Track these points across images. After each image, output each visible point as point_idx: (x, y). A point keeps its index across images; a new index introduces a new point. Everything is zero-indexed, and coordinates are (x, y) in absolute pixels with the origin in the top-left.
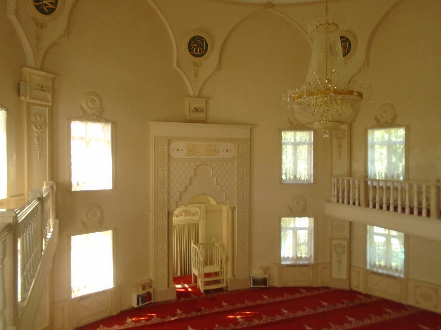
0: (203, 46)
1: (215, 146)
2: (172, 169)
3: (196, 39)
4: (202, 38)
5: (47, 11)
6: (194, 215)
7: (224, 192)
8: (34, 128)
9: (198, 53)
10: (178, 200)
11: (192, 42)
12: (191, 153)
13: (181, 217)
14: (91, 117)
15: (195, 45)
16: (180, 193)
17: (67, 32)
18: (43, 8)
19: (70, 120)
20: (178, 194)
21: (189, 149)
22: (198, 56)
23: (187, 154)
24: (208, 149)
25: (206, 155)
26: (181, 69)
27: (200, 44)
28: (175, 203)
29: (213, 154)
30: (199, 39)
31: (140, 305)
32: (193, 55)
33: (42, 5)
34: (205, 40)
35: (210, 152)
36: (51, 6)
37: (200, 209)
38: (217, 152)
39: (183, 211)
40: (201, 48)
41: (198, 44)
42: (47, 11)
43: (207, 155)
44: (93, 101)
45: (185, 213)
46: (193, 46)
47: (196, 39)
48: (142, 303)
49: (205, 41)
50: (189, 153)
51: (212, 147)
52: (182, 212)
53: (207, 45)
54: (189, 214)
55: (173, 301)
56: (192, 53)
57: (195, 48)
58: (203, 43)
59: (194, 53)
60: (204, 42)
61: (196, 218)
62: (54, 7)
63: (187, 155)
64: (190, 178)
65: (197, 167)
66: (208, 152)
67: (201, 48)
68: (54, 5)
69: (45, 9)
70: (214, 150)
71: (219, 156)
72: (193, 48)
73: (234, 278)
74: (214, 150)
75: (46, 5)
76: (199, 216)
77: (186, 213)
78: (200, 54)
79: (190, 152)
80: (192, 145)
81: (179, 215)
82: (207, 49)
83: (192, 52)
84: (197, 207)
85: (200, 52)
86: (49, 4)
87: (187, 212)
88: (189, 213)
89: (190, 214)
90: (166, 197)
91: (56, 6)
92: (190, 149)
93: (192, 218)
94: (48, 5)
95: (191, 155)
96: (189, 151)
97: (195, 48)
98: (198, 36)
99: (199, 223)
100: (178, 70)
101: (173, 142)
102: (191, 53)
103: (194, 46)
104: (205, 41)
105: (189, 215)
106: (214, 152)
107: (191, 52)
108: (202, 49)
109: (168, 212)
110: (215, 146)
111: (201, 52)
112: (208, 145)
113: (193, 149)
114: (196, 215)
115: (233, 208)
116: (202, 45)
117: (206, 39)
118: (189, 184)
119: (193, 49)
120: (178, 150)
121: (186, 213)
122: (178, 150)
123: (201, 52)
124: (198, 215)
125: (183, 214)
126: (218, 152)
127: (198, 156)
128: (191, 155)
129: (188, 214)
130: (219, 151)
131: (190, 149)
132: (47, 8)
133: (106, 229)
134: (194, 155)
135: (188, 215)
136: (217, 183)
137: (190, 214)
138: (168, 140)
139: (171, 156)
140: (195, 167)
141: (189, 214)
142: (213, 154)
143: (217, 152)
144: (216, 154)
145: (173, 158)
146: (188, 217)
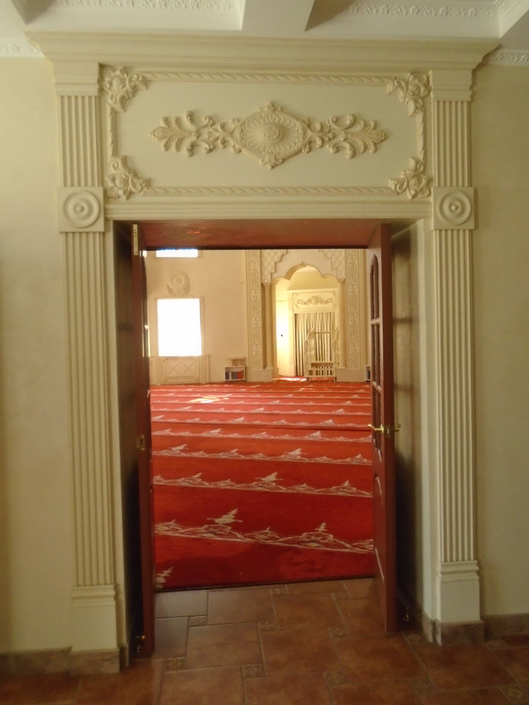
6: (327, 302)
10: (273, 271)
16: (276, 263)
20: (273, 264)
31: (230, 379)
39: (313, 297)
45: (315, 300)
48: (233, 378)
52: (311, 299)
54: (320, 301)
61: (330, 306)
73: (344, 368)
76: (333, 304)
77: (317, 299)
87: (318, 299)
88: (321, 300)
89: (322, 301)
90: (258, 267)
99: (334, 313)
105: (320, 302)
109: (262, 285)
114: (329, 302)
115: (343, 281)
121: (317, 299)
124: (332, 302)
129: (319, 301)
133: (193, 297)
135: (319, 302)
137: (322, 301)
141: (320, 301)
146: (319, 305)
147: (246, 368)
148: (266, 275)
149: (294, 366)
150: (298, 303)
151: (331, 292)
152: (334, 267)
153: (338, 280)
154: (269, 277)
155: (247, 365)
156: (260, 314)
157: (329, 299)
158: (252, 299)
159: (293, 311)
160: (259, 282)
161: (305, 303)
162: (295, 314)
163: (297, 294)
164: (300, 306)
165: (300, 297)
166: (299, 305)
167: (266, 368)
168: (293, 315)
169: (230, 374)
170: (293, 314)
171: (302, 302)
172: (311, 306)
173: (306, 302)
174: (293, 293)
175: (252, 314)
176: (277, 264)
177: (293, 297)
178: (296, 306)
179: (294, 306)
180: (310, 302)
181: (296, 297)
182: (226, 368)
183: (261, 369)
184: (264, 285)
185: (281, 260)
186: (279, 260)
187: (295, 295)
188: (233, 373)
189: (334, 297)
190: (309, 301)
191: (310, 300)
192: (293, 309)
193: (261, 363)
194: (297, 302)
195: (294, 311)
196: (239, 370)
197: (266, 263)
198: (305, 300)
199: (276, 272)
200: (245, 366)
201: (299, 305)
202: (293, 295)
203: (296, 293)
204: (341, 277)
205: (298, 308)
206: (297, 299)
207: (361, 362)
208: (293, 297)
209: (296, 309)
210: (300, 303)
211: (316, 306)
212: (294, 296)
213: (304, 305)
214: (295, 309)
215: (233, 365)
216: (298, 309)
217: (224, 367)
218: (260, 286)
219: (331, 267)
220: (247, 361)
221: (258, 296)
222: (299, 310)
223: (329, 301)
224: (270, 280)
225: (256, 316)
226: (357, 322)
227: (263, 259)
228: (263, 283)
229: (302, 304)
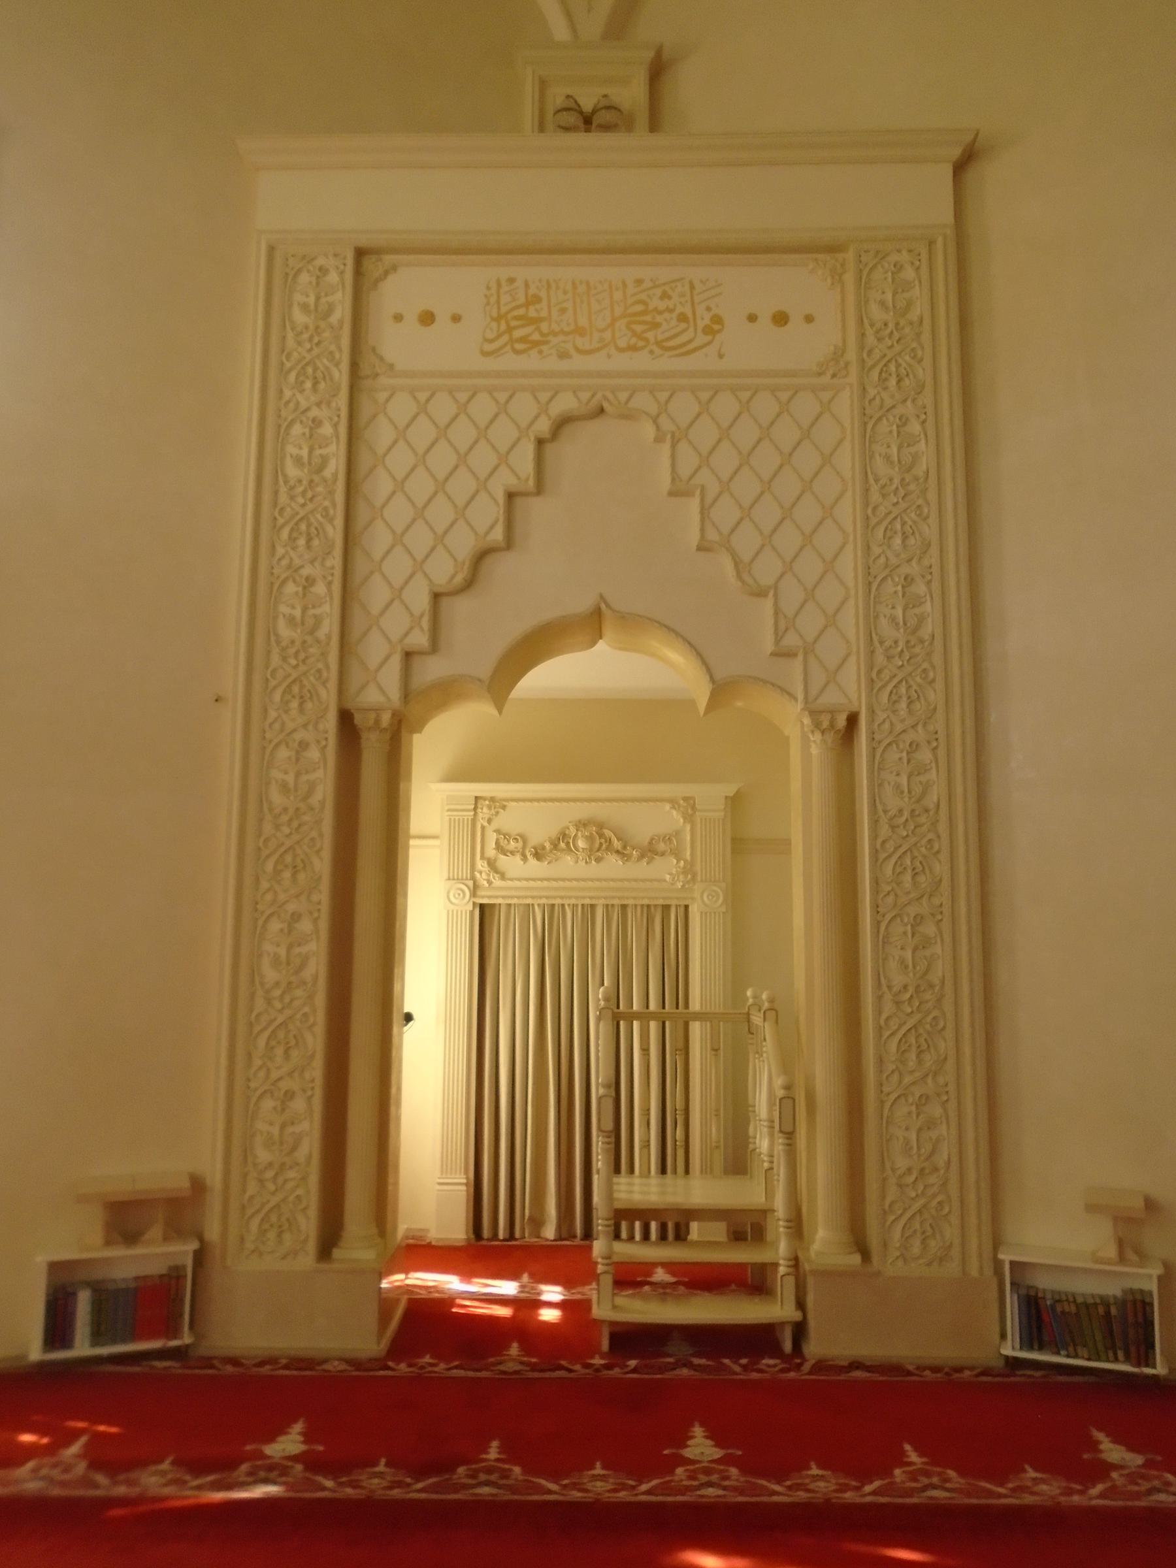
1: (692, 287)
2: (381, 434)
6: (649, 851)
7: (768, 603)
10: (419, 639)
12: (517, 334)
13: (569, 859)
16: (436, 597)
20: (420, 601)
21: (504, 310)
23: (491, 341)
24: (640, 308)
25: (621, 350)
28: (396, 662)
29: (671, 343)
35: (655, 325)
37: (689, 818)
38: (707, 330)
39: (582, 824)
43: (633, 348)
45: (590, 839)
48: (97, 1337)
50: (506, 338)
51: (665, 296)
52: (573, 832)
54: (617, 844)
55: (335, 1366)
61: (666, 869)
63: (488, 347)
64: (511, 496)
65: (562, 424)
66: (638, 328)
70: (682, 318)
71: (721, 356)
74: (682, 318)
76: (682, 863)
77: (601, 835)
79: (510, 330)
80: (527, 285)
81: (555, 846)
84: (667, 806)
87: (607, 833)
89: (625, 847)
90: (329, 612)
92: (515, 313)
93: (640, 869)
95: (519, 346)
96: (503, 327)
99: (687, 907)
101: (395, 268)
105: (618, 852)
106: (683, 325)
109: (346, 719)
110: (692, 287)
112: (639, 282)
113: (532, 313)
114: (663, 854)
115: (841, 722)
118: (498, 535)
120: (428, 318)
121: (601, 835)
122: (428, 318)
124: (677, 854)
125: (581, 844)
126: (716, 327)
127: (563, 355)
128: (518, 352)
130: (717, 319)
131: (515, 313)
134: (540, 352)
135: (610, 848)
136: (712, 535)
137: (625, 847)
138: (361, 254)
139: (381, 359)
140: (543, 426)
141: (617, 844)
142: (671, 343)
143: (707, 330)
144: (701, 339)
145: (391, 366)
146: (612, 866)
147: (200, 1257)
148: (373, 662)
149: (467, 1184)
150: (498, 847)
151: (673, 802)
152: (791, 640)
153: (814, 713)
154: (391, 676)
155: (213, 1233)
156: (323, 895)
157: (667, 839)
158: (276, 798)
159: (474, 894)
160: (329, 696)
161: (538, 855)
162: (482, 907)
163: (497, 804)
164: (512, 864)
165: (510, 820)
166: (503, 861)
167: (337, 1253)
168: (472, 913)
169: (83, 1302)
170: (474, 904)
171: (525, 842)
172: (568, 865)
173: (544, 848)
174: (477, 798)
175: (269, 897)
176: (445, 602)
177: (474, 821)
178: (492, 864)
179: (481, 865)
180: (563, 845)
181: (489, 821)
182: (55, 1268)
183: (307, 1259)
184: (358, 719)
185: (469, 584)
186: (459, 579)
187: (489, 807)
188: (105, 1296)
189: (688, 827)
190: (561, 842)
191: (564, 835)
192: (473, 878)
193: (309, 1225)
194: (497, 843)
195: (480, 893)
196: (156, 1268)
197: (376, 594)
198: (540, 834)
199: (434, 646)
200: (193, 1245)
201: (503, 861)
202: (475, 809)
203: (492, 799)
204: (831, 698)
205: (503, 877)
206: (498, 831)
207: (963, 1226)
208: (474, 821)
209: (489, 882)
210: (512, 853)
211: (594, 869)
212: (484, 812)
213: (532, 861)
214: (482, 880)
215: (108, 1243)
216: (497, 882)
217: (42, 1259)
218: (331, 723)
219: (778, 638)
220: (214, 1203)
221: (312, 787)
222: (509, 883)
223: (662, 846)
224: (395, 694)
225: (291, 907)
226: (940, 969)
227: (361, 565)
228: (349, 705)
229: (524, 858)
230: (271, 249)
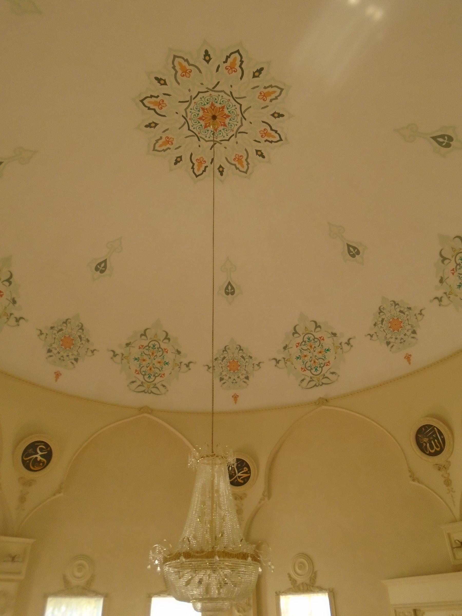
0: (436, 436)
3: (423, 431)
4: (430, 426)
5: (242, 482)
8: (236, 611)
9: (436, 450)
11: (420, 437)
14: (301, 588)
15: (426, 440)
17: (268, 493)
18: (238, 481)
19: (278, 594)
22: (436, 454)
26: (419, 482)
27: (432, 435)
30: (426, 429)
32: (431, 454)
33: (236, 478)
34: (435, 427)
36: (245, 475)
40: (436, 440)
41: (428, 437)
42: (242, 482)
44: (302, 565)
46: (424, 442)
47: (423, 431)
49: (435, 429)
53: (441, 434)
56: (428, 453)
57: (428, 444)
58: (435, 433)
59: (429, 451)
60: (435, 430)
62: (249, 475)
67: (436, 440)
68: (248, 473)
69: (240, 481)
72: (424, 445)
75: (239, 477)
78: (438, 449)
82: (444, 438)
83: (427, 451)
85: (437, 447)
86: (242, 475)
91: (250, 473)
94: (243, 476)
97: (428, 444)
98: (424, 426)
100: (416, 483)
101: (424, 613)
102: (427, 453)
103: (425, 441)
104: (435, 429)
107: (425, 451)
108: (437, 440)
111: (439, 445)
116: (434, 436)
117: (436, 426)
119: (426, 446)
123: (439, 445)
132: (242, 479)
138: (415, 611)
230: (395, 611)
